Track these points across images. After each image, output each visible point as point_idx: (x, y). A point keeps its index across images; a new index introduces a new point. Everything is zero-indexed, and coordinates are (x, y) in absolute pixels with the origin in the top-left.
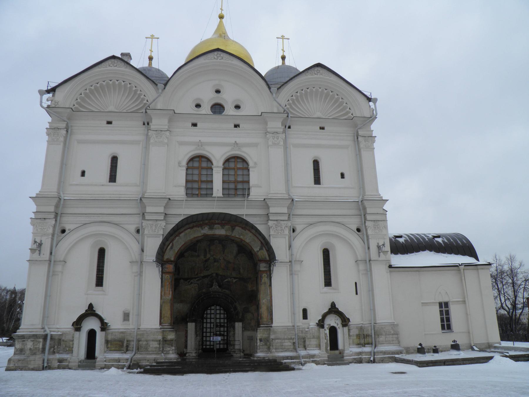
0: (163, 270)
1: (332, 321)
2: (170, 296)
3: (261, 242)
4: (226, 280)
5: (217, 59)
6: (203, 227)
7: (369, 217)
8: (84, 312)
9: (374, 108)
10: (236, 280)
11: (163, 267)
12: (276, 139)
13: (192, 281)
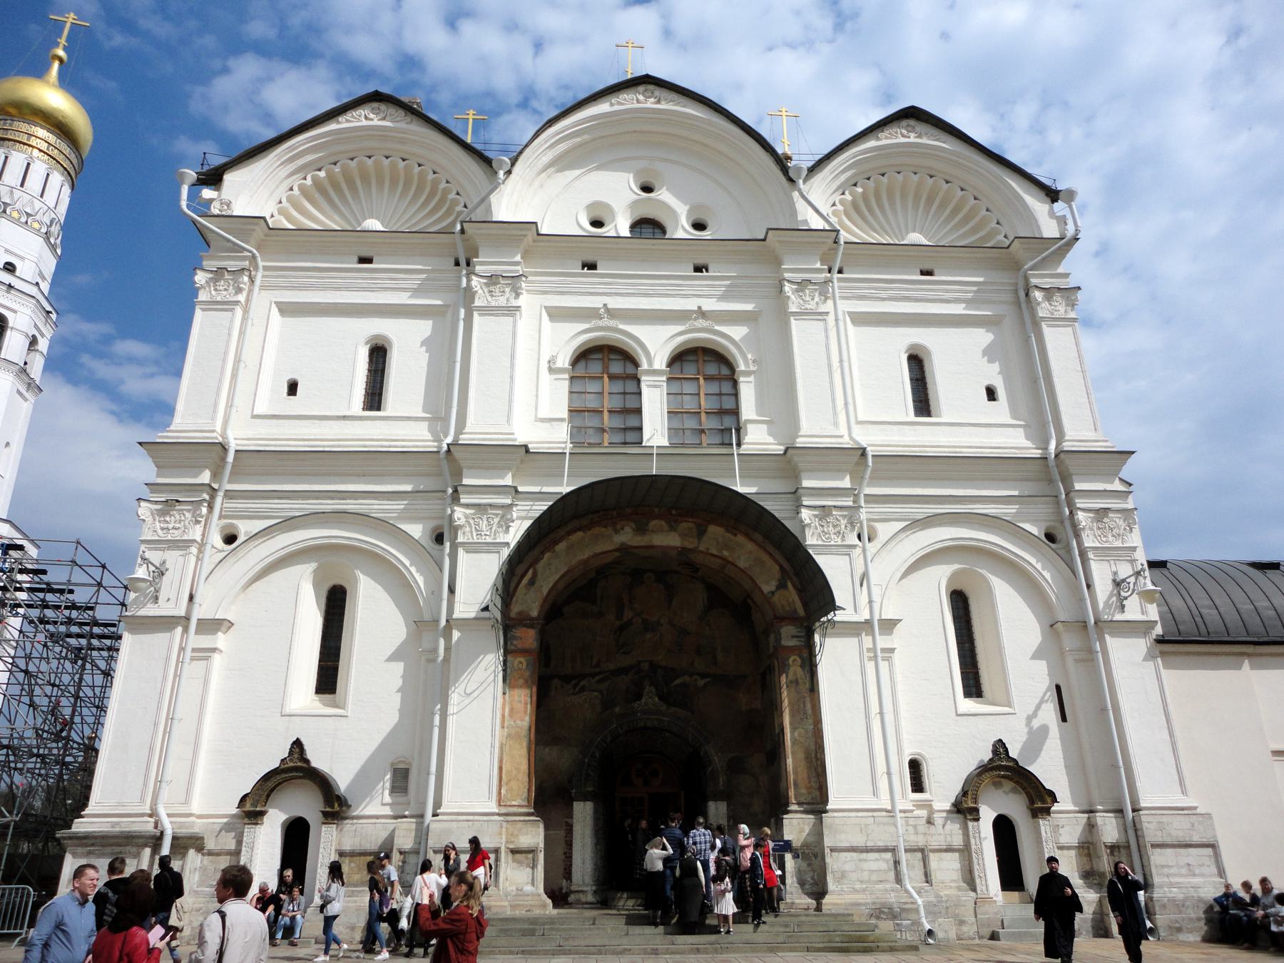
0: (509, 643)
2: (527, 718)
3: (781, 566)
4: (677, 682)
6: (618, 527)
7: (1080, 503)
8: (275, 764)
10: (707, 680)
11: (509, 636)
12: (808, 298)
13: (582, 683)
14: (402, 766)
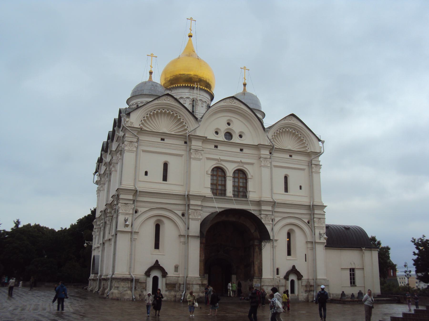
1: (292, 277)
5: (232, 103)
7: (316, 216)
9: (322, 147)
12: (266, 162)
14: (176, 266)
